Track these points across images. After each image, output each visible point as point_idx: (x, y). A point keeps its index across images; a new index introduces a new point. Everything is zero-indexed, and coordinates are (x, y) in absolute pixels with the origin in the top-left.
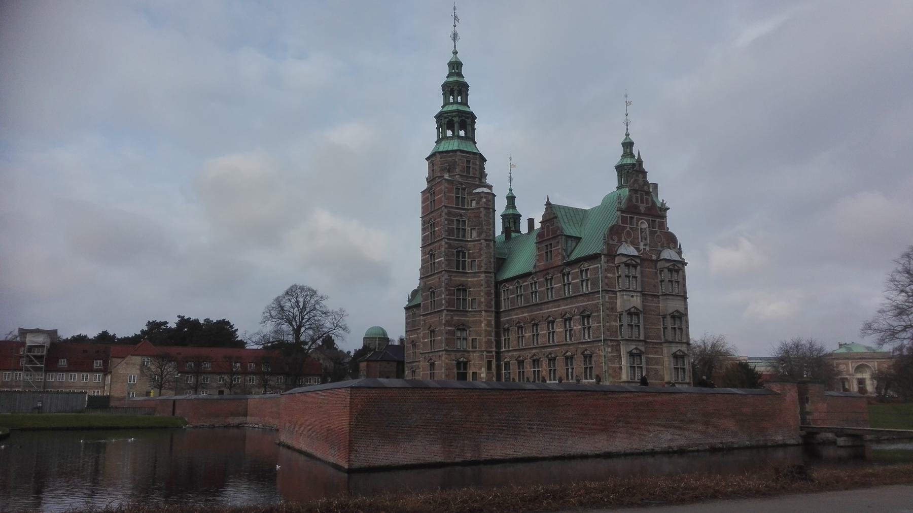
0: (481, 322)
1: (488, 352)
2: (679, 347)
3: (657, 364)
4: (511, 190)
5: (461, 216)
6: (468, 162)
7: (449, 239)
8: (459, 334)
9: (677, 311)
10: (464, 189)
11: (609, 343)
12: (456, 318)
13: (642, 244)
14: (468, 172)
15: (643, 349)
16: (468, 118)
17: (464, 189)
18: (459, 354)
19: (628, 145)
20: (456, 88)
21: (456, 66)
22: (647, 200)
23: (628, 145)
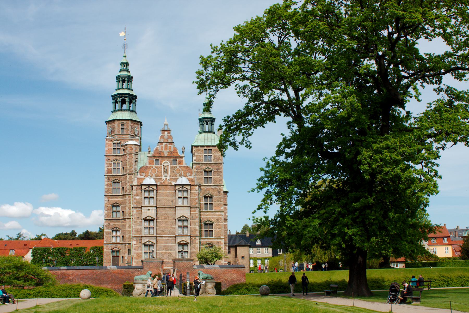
0: (126, 225)
1: (128, 244)
2: (184, 238)
3: (171, 249)
5: (116, 160)
6: (123, 125)
7: (107, 176)
8: (114, 233)
9: (183, 216)
10: (120, 143)
11: (135, 239)
12: (112, 224)
13: (163, 176)
14: (123, 132)
15: (154, 241)
17: (120, 143)
18: (113, 246)
22: (170, 148)
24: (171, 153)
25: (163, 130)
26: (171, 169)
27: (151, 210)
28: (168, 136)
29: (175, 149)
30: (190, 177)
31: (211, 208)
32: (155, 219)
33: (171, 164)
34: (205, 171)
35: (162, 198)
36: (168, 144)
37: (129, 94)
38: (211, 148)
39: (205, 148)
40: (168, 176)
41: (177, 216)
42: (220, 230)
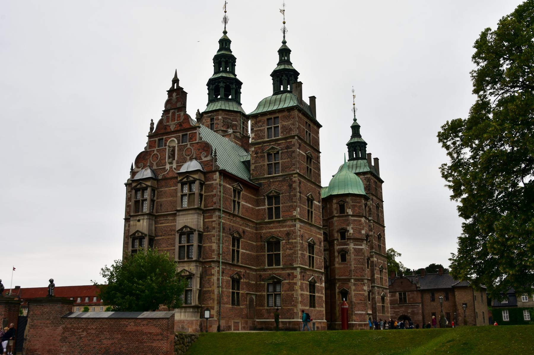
4: (355, 120)
9: (186, 227)
16: (220, 82)
19: (284, 52)
20: (225, 60)
21: (225, 43)
22: (179, 116)
23: (284, 52)
24: (180, 124)
25: (170, 92)
26: (179, 150)
27: (141, 221)
28: (177, 98)
29: (188, 117)
30: (206, 159)
31: (278, 216)
32: (146, 235)
33: (179, 143)
34: (269, 155)
35: (164, 199)
36: (176, 111)
37: (222, 77)
38: (277, 115)
39: (269, 117)
40: (174, 162)
41: (179, 227)
42: (291, 251)
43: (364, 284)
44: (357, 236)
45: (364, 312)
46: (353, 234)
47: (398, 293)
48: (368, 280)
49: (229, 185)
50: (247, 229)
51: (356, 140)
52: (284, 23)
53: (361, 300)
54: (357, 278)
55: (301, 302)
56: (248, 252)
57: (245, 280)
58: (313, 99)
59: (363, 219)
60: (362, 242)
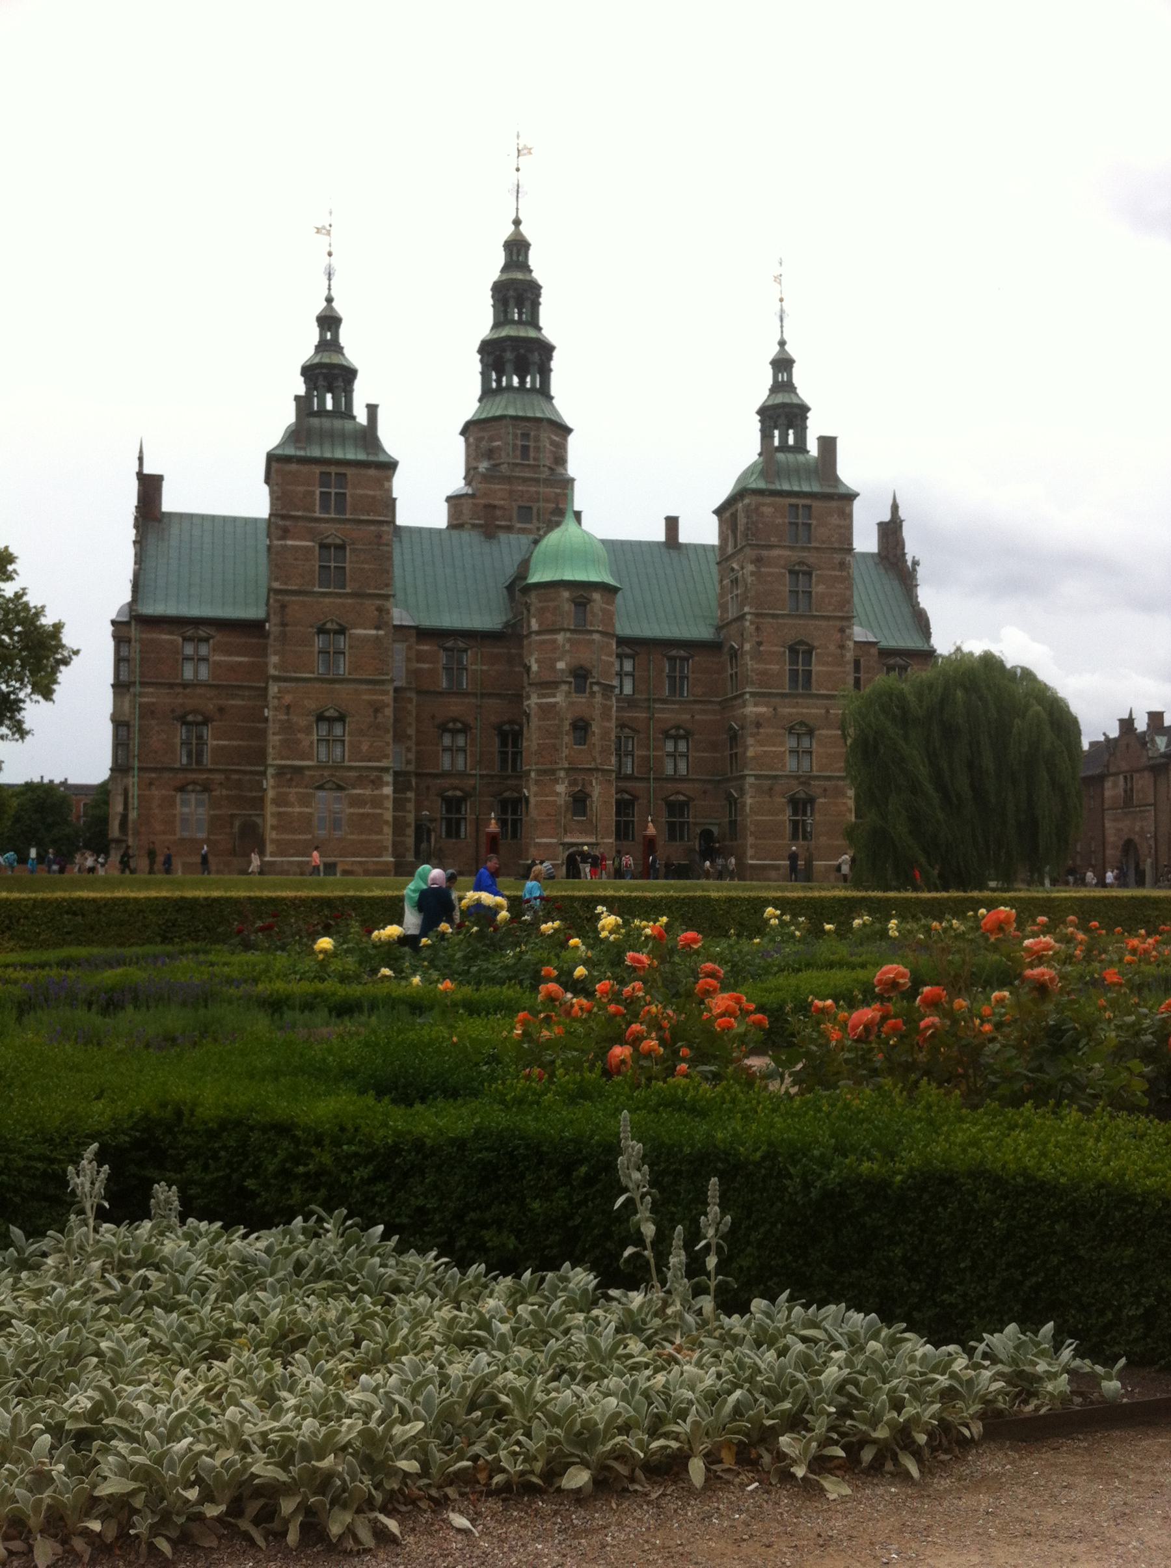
19: (329, 322)
20: (516, 293)
21: (517, 249)
23: (329, 322)
43: (556, 781)
44: (548, 677)
45: (554, 841)
46: (538, 672)
47: (1121, 777)
48: (567, 770)
49: (171, 633)
50: (233, 702)
51: (780, 399)
52: (330, 254)
53: (548, 815)
54: (545, 767)
55: (273, 828)
56: (235, 743)
57: (224, 792)
58: (372, 409)
59: (560, 637)
60: (557, 688)
